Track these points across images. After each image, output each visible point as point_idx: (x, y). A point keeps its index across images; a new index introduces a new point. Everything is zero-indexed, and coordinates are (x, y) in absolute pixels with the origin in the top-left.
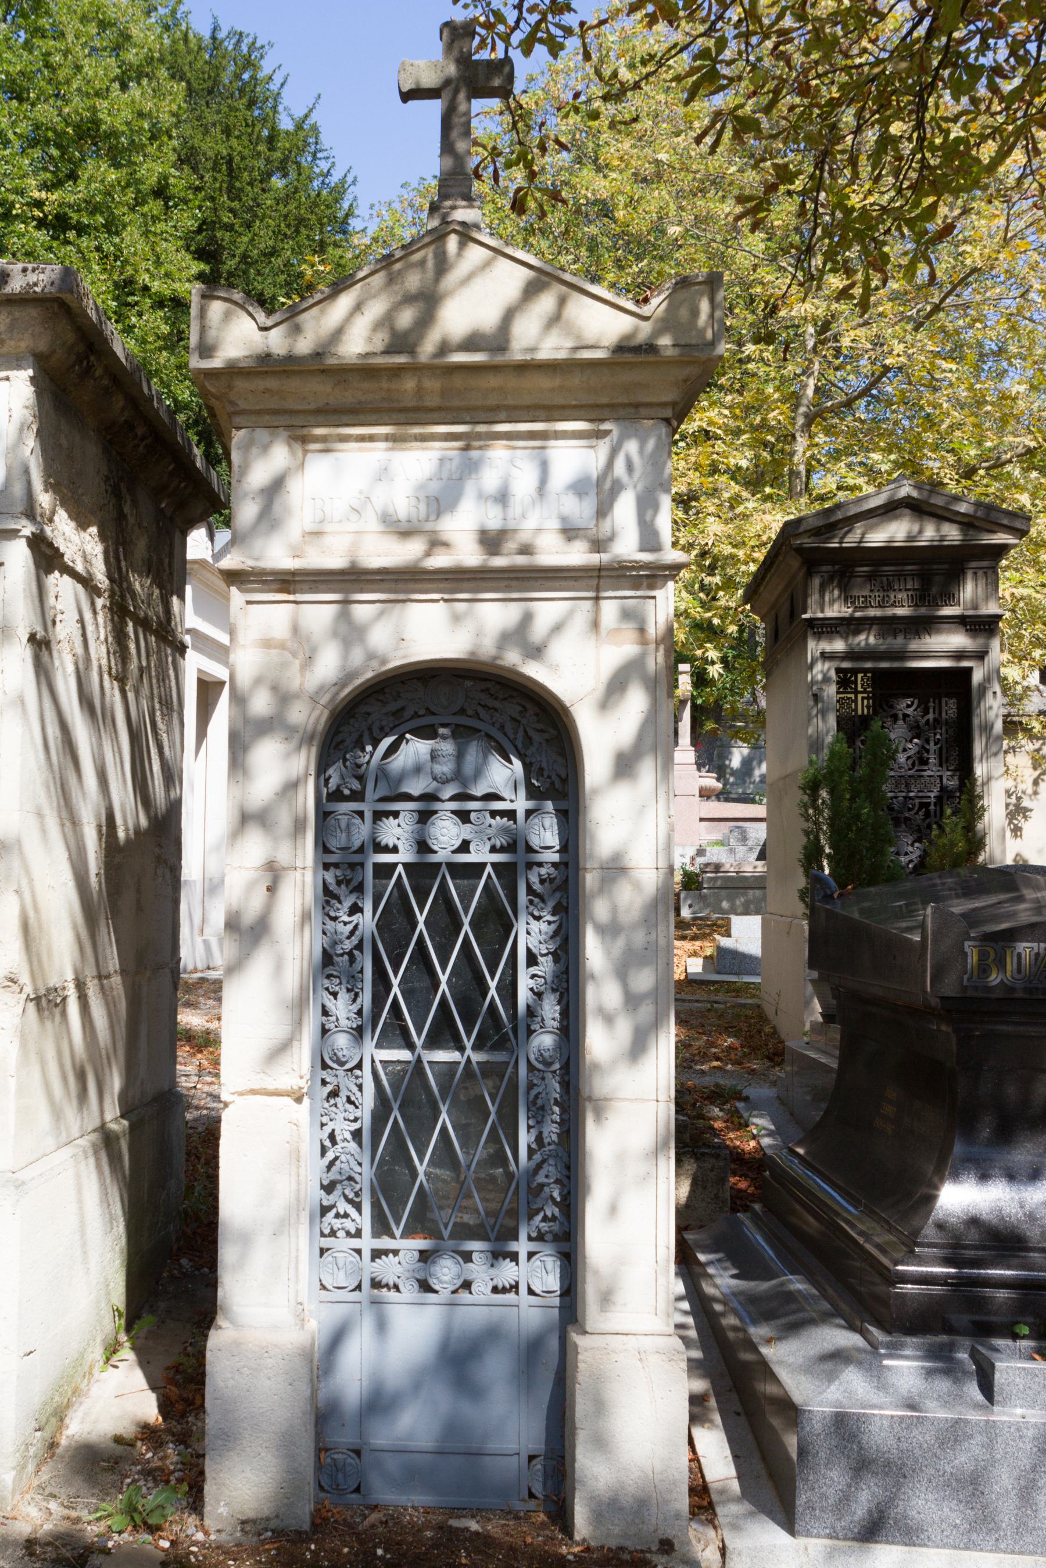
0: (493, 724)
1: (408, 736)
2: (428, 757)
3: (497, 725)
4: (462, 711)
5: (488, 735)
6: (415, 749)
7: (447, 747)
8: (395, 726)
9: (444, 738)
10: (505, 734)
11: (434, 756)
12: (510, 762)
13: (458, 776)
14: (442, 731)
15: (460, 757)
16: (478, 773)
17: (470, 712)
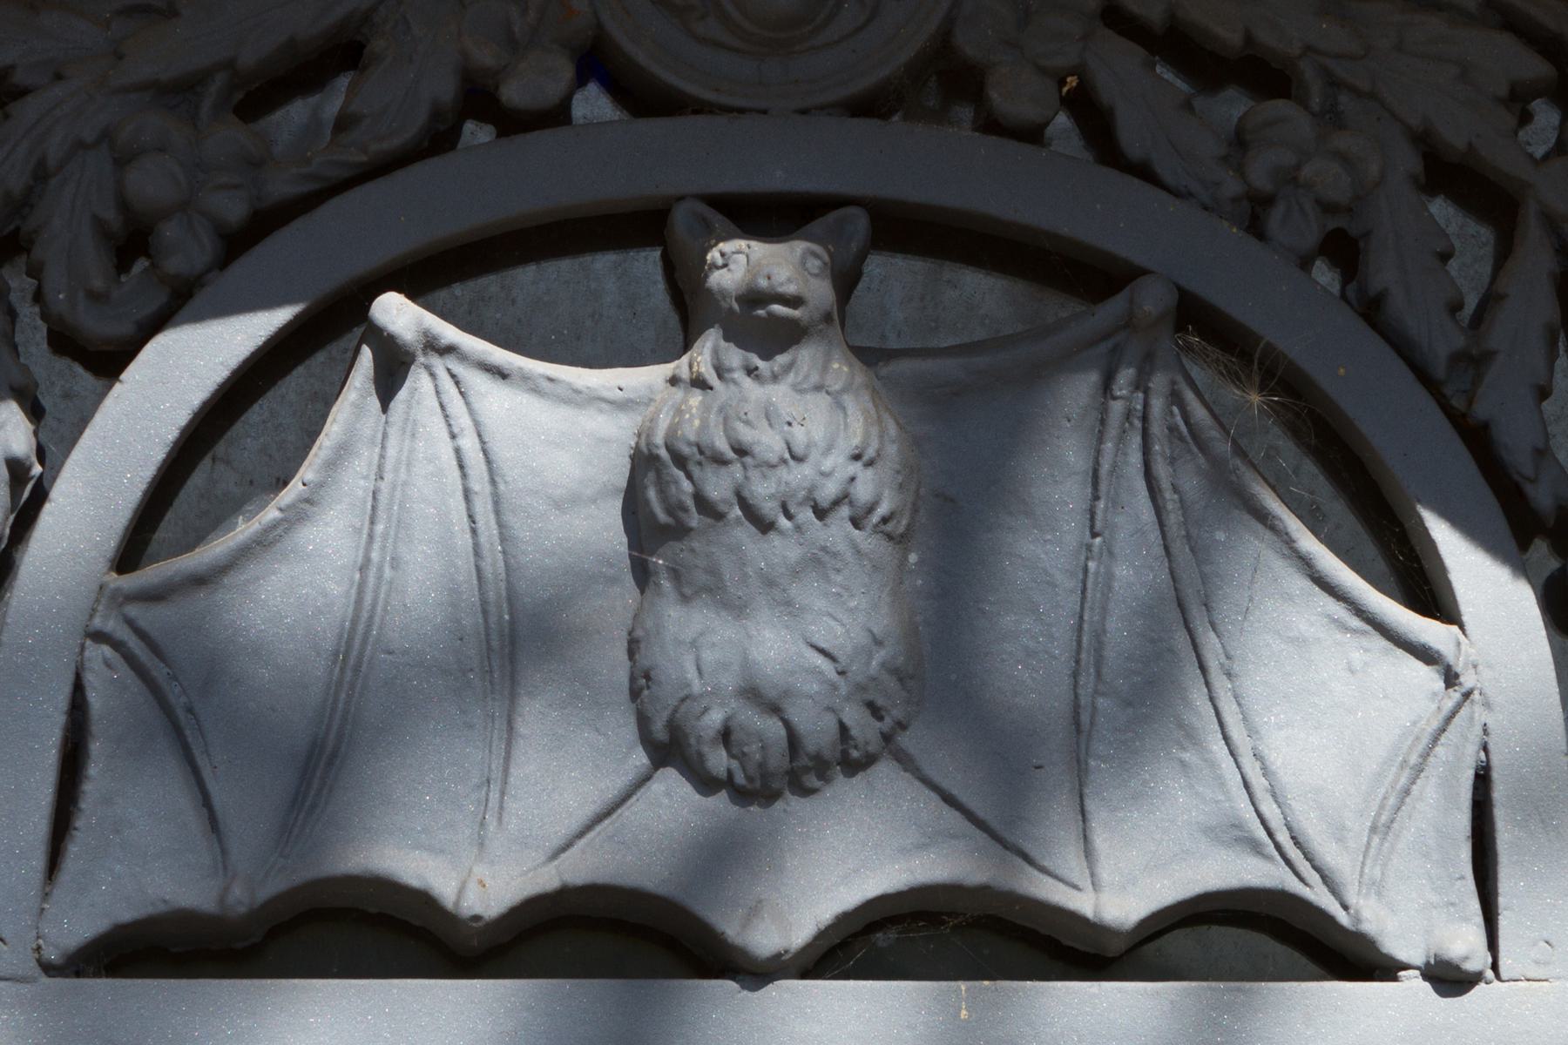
0: (1254, 215)
1: (396, 312)
2: (604, 528)
3: (1297, 226)
4: (946, 80)
5: (1199, 321)
6: (477, 449)
7: (811, 424)
8: (265, 222)
9: (764, 329)
10: (1372, 310)
11: (667, 512)
12: (1427, 592)
13: (933, 699)
14: (737, 262)
15: (947, 524)
16: (1148, 683)
17: (1017, 92)
